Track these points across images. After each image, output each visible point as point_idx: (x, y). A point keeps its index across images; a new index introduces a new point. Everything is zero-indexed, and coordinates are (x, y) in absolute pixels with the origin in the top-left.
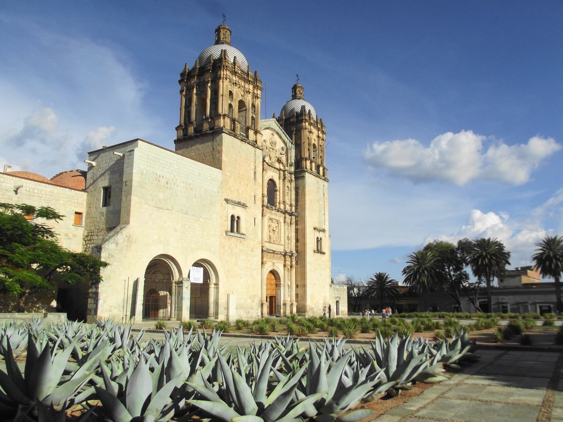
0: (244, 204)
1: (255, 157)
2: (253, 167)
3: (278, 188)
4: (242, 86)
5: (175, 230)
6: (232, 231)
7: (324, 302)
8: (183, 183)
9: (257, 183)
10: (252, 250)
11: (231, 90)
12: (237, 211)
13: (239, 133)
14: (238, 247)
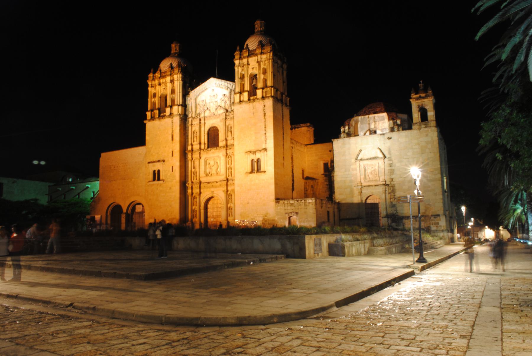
0: (162, 160)
1: (172, 124)
2: (170, 132)
3: (220, 131)
4: (163, 83)
5: (119, 189)
6: (154, 180)
7: (264, 219)
8: (122, 164)
9: (174, 141)
10: (171, 188)
11: (155, 91)
12: (157, 166)
13: (157, 116)
14: (159, 189)
